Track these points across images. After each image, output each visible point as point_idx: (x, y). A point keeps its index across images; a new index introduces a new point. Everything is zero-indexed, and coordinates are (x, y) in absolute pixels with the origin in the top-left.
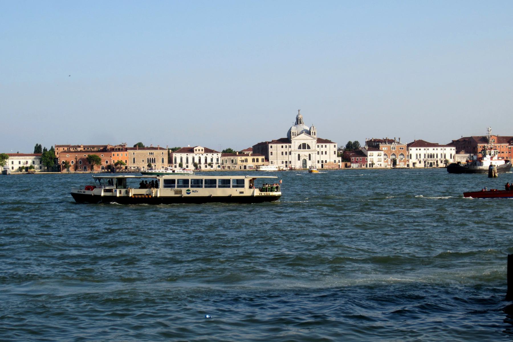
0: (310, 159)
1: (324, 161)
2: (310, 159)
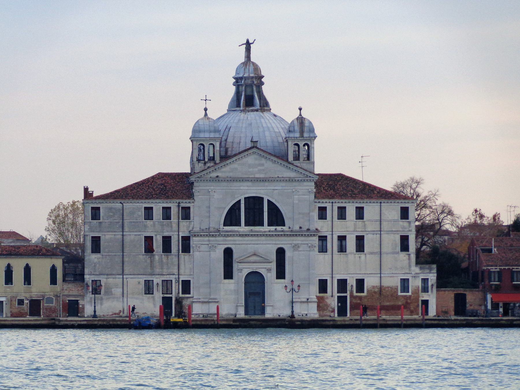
0: (281, 274)
1: (352, 283)
2: (281, 274)
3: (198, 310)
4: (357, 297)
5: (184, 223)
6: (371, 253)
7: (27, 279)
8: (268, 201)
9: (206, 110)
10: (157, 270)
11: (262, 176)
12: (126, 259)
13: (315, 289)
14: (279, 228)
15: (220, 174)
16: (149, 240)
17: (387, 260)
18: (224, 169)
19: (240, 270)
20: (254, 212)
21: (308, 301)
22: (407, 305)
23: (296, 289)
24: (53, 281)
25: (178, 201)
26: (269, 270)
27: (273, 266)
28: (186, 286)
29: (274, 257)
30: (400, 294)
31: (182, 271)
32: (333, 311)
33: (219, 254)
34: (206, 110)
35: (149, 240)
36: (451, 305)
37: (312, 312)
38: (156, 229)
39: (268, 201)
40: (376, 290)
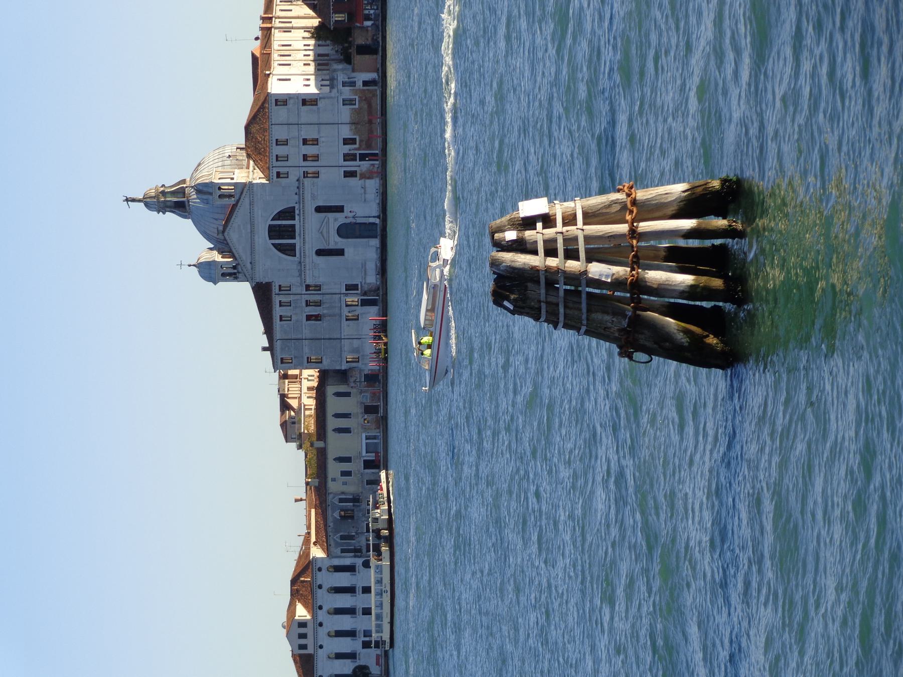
0: (340, 209)
1: (347, 149)
2: (340, 209)
3: (372, 279)
4: (360, 144)
5: (294, 290)
6: (319, 132)
7: (346, 416)
8: (273, 219)
9: (190, 266)
10: (337, 311)
11: (249, 226)
12: (327, 337)
13: (352, 181)
14: (297, 212)
15: (249, 261)
16: (309, 318)
17: (325, 118)
18: (244, 258)
19: (336, 243)
20: (282, 232)
21: (364, 188)
22: (367, 100)
23: (352, 214)
24: (347, 394)
25: (274, 296)
26: (336, 220)
27: (331, 216)
28: (351, 287)
29: (323, 215)
30: (357, 106)
31: (338, 291)
32: (373, 165)
33: (322, 260)
34: (190, 266)
35: (309, 318)
36: (367, 57)
37: (373, 185)
38: (300, 314)
39: (273, 219)
40: (353, 127)
